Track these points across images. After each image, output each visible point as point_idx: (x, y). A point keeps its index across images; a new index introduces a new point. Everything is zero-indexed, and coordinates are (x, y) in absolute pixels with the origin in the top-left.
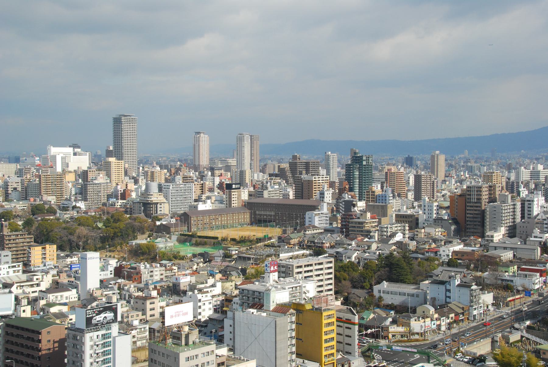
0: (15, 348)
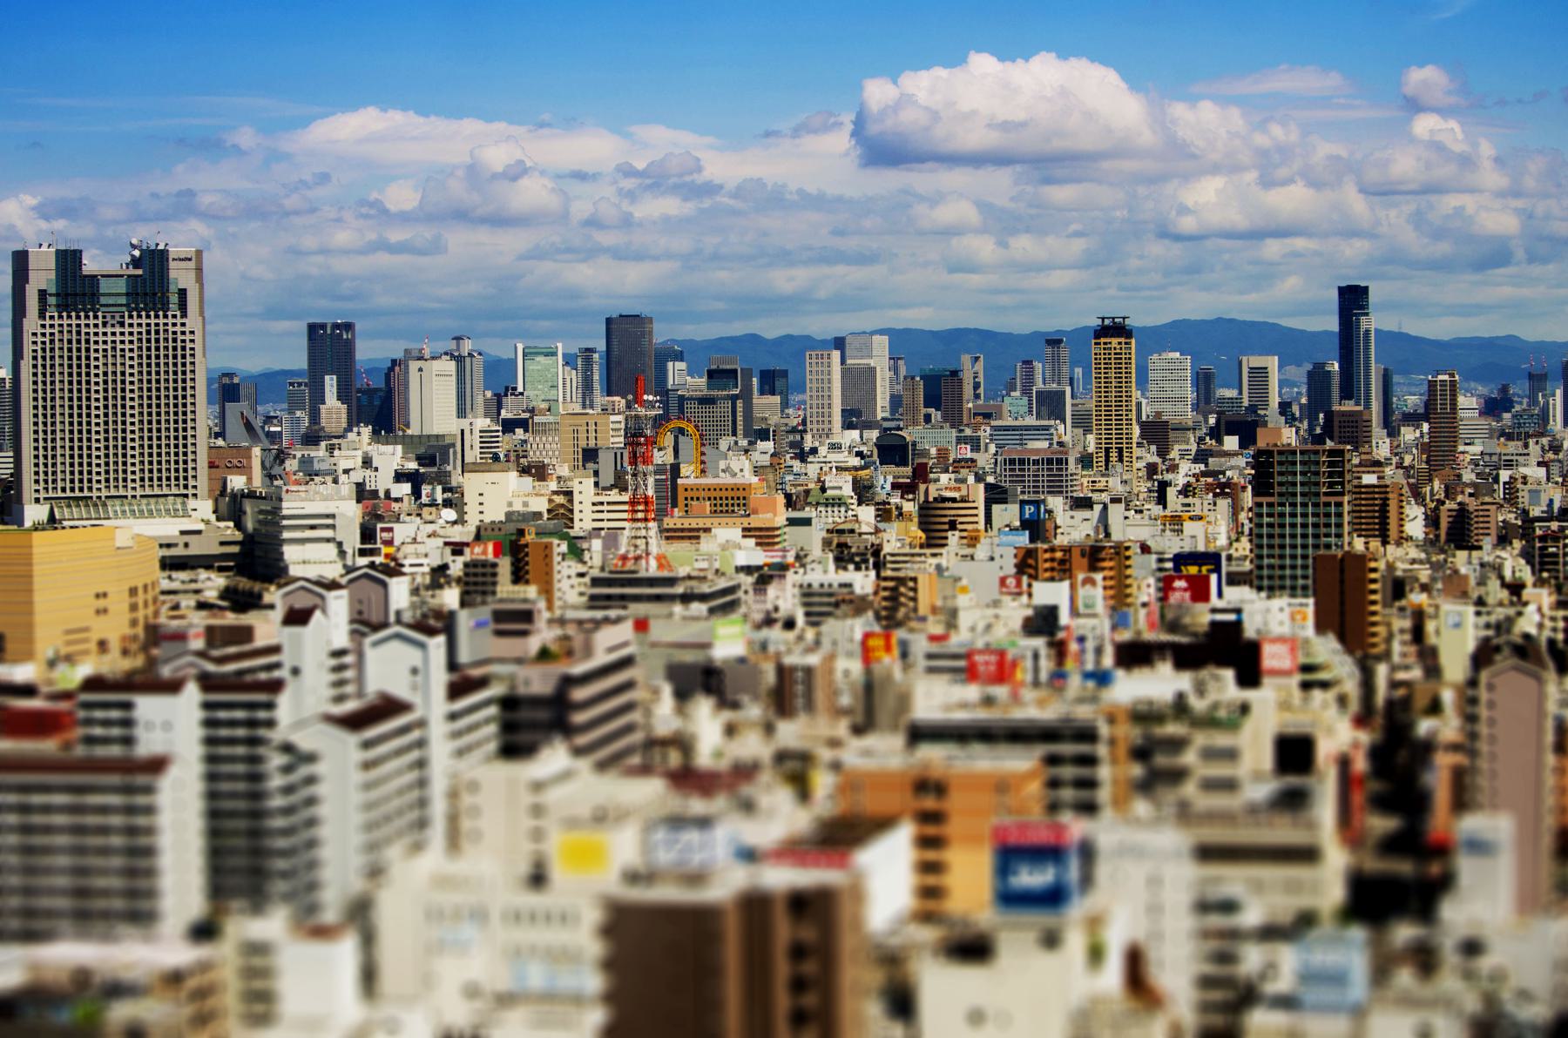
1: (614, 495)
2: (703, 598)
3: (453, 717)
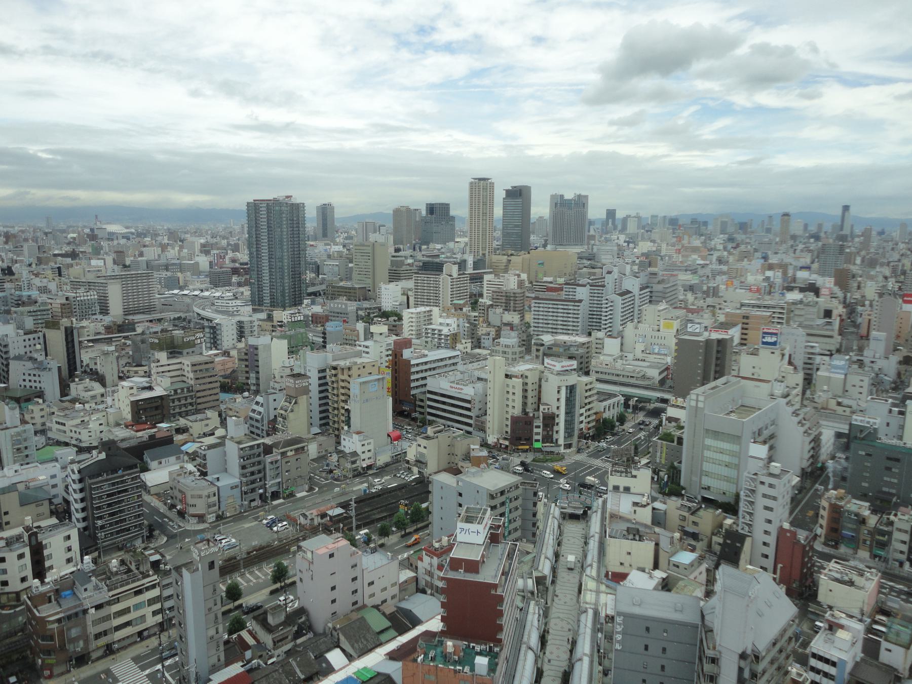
3: (640, 295)
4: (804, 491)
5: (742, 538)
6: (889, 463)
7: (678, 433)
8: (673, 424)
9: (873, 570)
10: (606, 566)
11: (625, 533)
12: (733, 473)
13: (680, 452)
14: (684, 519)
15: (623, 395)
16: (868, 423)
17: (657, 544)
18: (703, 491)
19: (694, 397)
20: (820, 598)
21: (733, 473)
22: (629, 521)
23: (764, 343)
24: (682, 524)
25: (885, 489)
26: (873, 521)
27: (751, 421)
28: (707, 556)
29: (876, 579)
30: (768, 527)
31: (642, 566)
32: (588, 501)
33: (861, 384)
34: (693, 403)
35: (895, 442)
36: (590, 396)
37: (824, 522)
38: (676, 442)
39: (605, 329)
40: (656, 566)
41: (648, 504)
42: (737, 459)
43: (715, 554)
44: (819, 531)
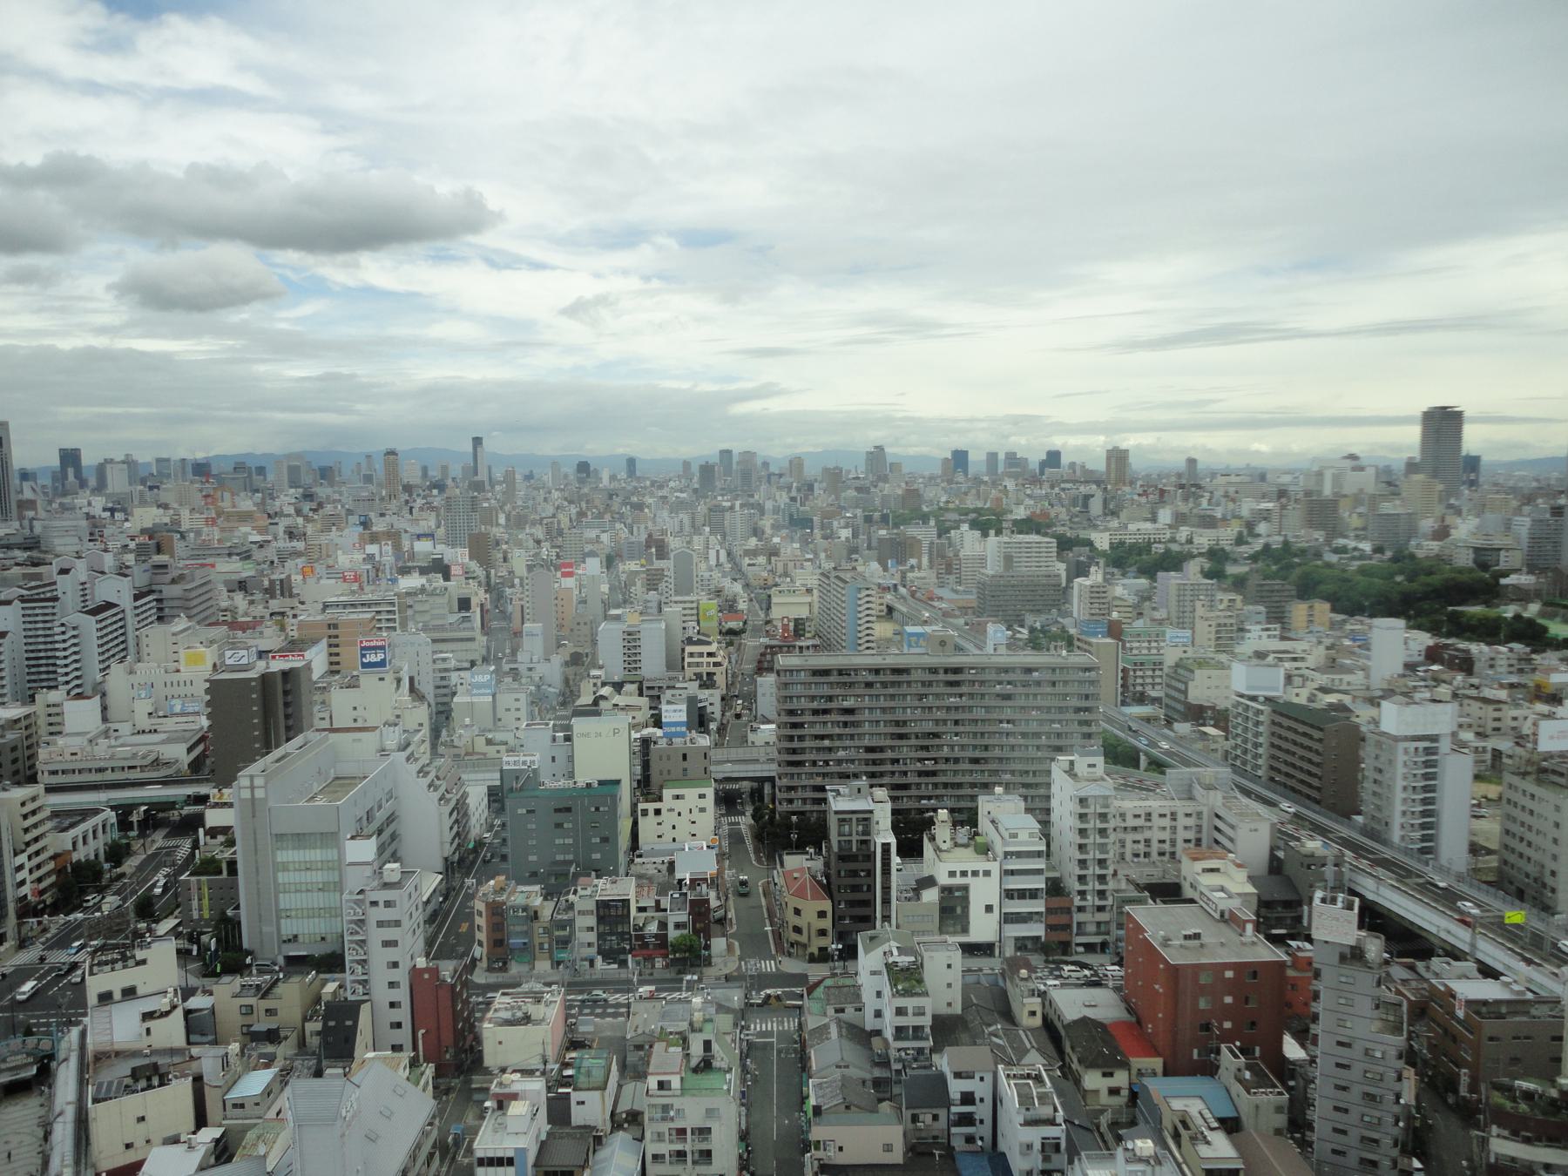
0: (1285, 745)
1: (197, 516)
2: (238, 554)
3: (136, 608)
4: (453, 893)
5: (352, 1010)
6: (559, 817)
7: (227, 855)
8: (221, 838)
9: (554, 987)
10: (94, 1166)
11: (129, 1081)
12: (331, 899)
13: (234, 887)
14: (249, 1010)
15: (113, 808)
16: (524, 763)
17: (198, 1079)
18: (285, 946)
19: (244, 782)
20: (489, 1061)
21: (331, 899)
22: (135, 1054)
23: (364, 665)
24: (248, 1020)
25: (560, 857)
26: (547, 910)
27: (350, 803)
28: (297, 1063)
29: (559, 999)
30: (396, 975)
31: (171, 1133)
32: (45, 1045)
33: (517, 705)
34: (246, 794)
35: (563, 783)
36: (35, 826)
37: (481, 936)
38: (225, 872)
39: (67, 683)
40: (201, 1121)
41: (174, 1007)
42: (336, 873)
43: (314, 1054)
44: (478, 951)
